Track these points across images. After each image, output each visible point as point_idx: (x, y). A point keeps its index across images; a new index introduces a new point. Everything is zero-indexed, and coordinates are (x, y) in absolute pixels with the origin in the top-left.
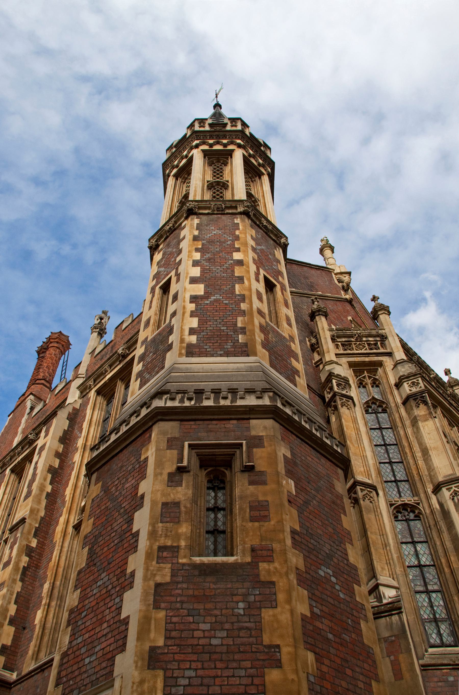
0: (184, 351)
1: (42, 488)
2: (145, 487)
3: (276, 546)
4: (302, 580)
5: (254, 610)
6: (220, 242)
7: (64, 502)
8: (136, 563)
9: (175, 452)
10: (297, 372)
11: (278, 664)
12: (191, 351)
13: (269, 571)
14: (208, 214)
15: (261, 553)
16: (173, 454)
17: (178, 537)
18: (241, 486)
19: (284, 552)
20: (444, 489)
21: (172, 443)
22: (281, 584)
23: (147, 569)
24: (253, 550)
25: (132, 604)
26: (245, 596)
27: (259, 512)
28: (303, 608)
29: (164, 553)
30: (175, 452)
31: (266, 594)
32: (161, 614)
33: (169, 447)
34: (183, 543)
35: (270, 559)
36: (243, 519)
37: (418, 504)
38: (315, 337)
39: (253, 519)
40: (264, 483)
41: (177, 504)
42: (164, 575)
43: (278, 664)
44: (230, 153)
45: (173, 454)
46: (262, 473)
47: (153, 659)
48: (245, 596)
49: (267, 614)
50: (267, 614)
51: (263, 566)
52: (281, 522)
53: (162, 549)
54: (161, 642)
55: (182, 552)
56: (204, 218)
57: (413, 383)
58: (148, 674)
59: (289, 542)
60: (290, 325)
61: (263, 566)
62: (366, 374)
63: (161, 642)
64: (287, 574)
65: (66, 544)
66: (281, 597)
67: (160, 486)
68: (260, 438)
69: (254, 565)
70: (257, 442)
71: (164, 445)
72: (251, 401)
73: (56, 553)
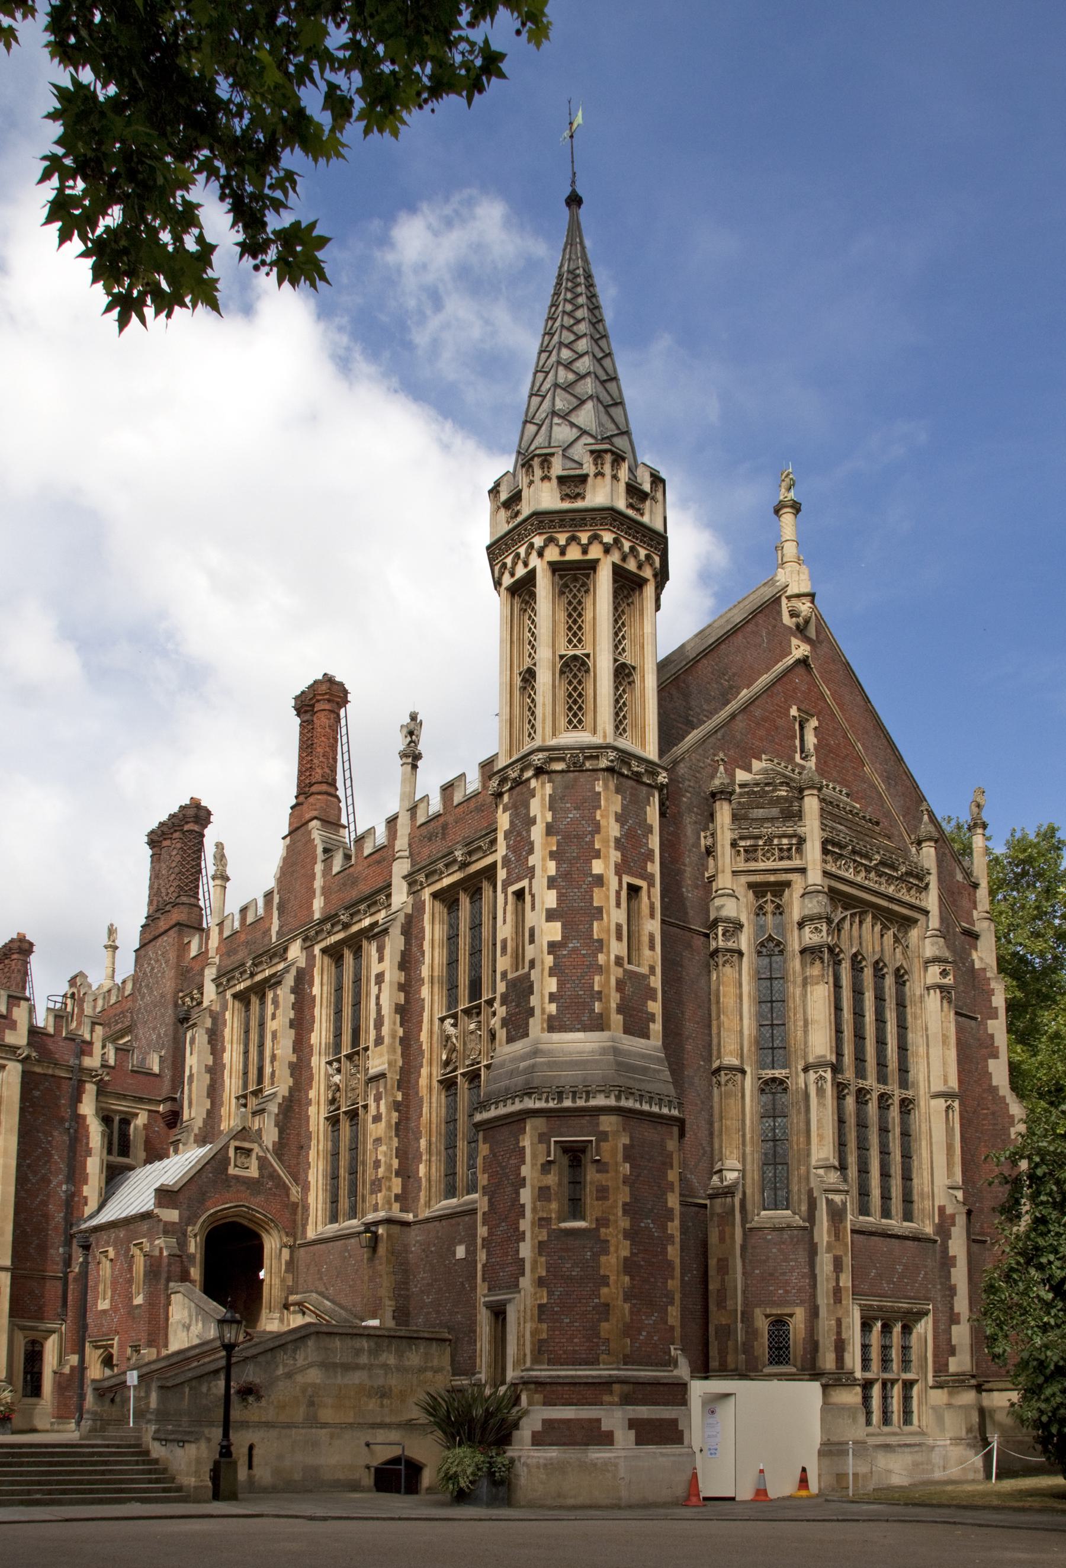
0: (545, 1025)
1: (393, 1035)
2: (525, 1171)
3: (612, 1218)
4: (627, 1235)
5: (596, 1256)
6: (577, 836)
7: (422, 1052)
8: (525, 1225)
9: (545, 1146)
10: (652, 1018)
11: (608, 1285)
12: (553, 1025)
13: (606, 1234)
14: (562, 771)
15: (603, 1222)
16: (542, 1147)
17: (550, 1211)
18: (591, 1175)
19: (616, 1221)
20: (811, 1072)
21: (543, 1138)
22: (613, 1241)
23: (532, 1233)
24: (597, 1220)
25: (526, 1250)
26: (592, 1248)
27: (603, 1193)
28: (625, 1253)
29: (542, 1222)
30: (545, 1146)
31: (604, 1247)
32: (543, 1259)
33: (540, 1142)
34: (553, 1216)
35: (607, 1226)
36: (592, 1199)
37: (787, 1078)
38: (713, 835)
39: (597, 1199)
40: (607, 1172)
41: (548, 1188)
42: (543, 1236)
43: (608, 1285)
44: (592, 566)
45: (542, 1147)
46: (606, 1164)
47: (540, 1282)
48: (592, 1248)
49: (603, 1259)
50: (603, 1259)
51: (603, 1230)
52: (616, 1201)
53: (540, 1219)
54: (544, 1274)
55: (553, 1222)
56: (558, 778)
57: (816, 928)
58: (539, 1290)
59: (620, 1213)
60: (652, 948)
61: (603, 1230)
62: (769, 896)
63: (544, 1274)
64: (617, 1236)
65: (434, 1100)
66: (612, 1249)
67: (536, 1174)
68: (605, 1133)
69: (597, 1229)
70: (603, 1136)
71: (536, 1140)
72: (600, 1101)
73: (425, 1110)
